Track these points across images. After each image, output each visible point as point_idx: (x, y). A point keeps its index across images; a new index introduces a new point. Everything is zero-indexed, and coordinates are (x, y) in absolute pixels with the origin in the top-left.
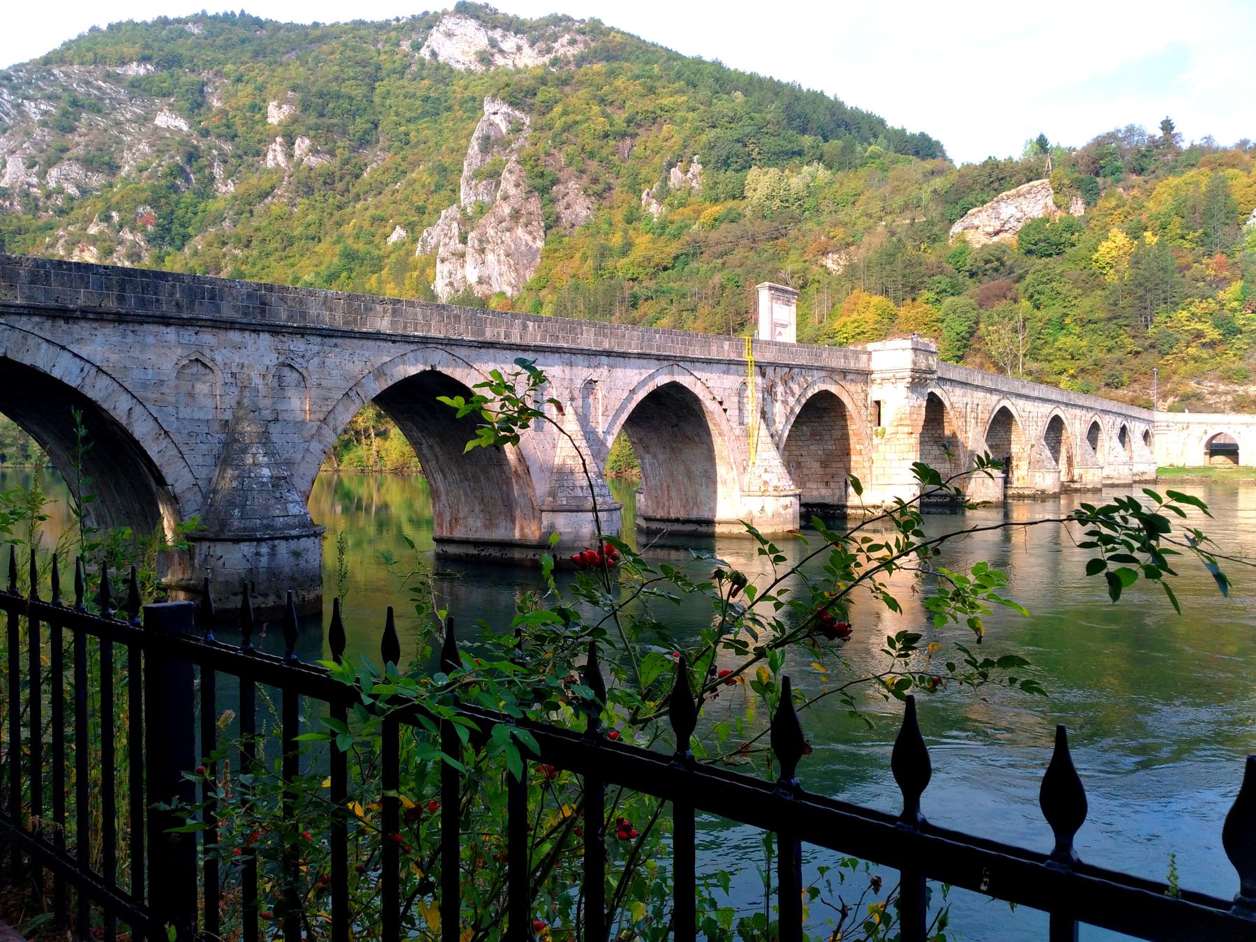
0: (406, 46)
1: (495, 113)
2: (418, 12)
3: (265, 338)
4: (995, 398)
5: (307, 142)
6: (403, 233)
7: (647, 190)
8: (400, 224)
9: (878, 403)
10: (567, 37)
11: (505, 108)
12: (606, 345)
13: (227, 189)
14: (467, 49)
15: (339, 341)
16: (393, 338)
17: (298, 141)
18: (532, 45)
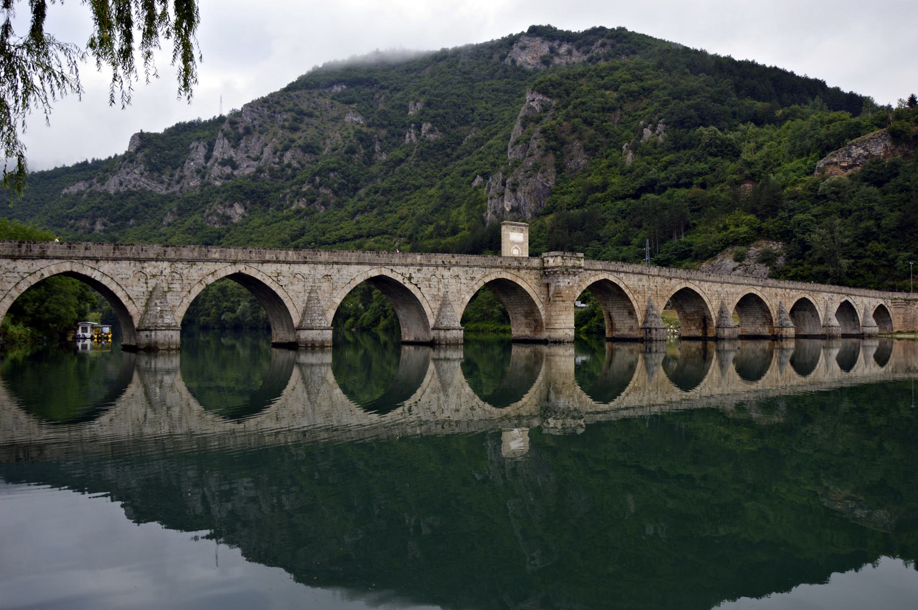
1: (533, 100)
2: (506, 35)
3: (166, 264)
5: (429, 125)
6: (482, 180)
7: (626, 144)
8: (479, 174)
9: (548, 285)
10: (600, 41)
11: (540, 97)
12: (335, 259)
14: (535, 56)
17: (424, 125)
18: (578, 49)
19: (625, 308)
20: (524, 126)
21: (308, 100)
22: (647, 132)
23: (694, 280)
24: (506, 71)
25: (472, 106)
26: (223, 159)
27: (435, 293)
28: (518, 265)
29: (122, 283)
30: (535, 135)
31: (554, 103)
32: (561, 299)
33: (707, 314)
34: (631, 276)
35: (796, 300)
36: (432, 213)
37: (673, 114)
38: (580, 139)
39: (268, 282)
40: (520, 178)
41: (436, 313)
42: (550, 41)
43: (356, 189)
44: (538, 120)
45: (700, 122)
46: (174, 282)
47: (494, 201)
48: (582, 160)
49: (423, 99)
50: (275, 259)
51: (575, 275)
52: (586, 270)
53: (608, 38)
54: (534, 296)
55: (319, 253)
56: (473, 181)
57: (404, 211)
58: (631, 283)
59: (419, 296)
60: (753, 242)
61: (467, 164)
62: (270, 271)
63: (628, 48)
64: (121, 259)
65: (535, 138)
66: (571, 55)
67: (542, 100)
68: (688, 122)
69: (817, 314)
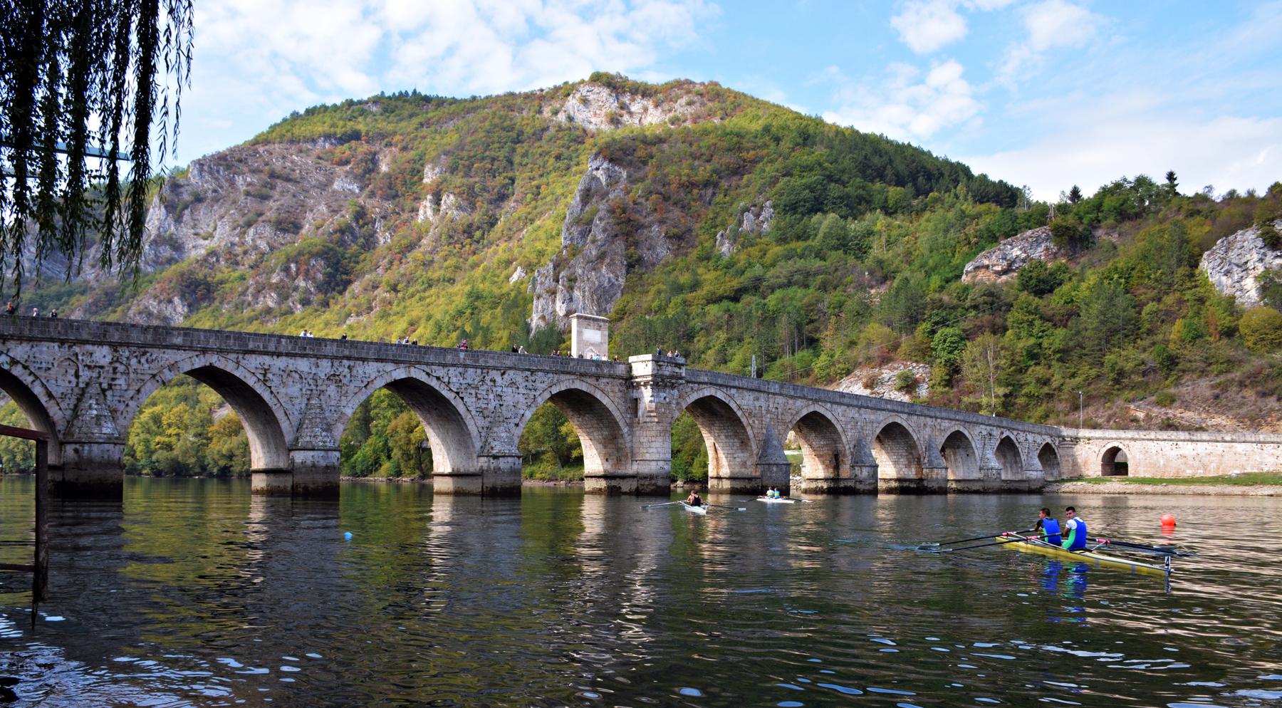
0: (547, 112)
1: (597, 169)
2: (559, 83)
3: (106, 350)
4: (799, 403)
5: (452, 197)
6: (523, 274)
8: (521, 265)
9: (636, 399)
10: (683, 101)
11: (605, 165)
12: (347, 353)
13: (384, 238)
15: (150, 350)
17: (444, 198)
18: (656, 106)
19: (736, 435)
21: (284, 157)
23: (825, 401)
25: (510, 174)
26: (159, 235)
27: (484, 406)
28: (595, 370)
29: (41, 374)
30: (601, 214)
33: (840, 447)
34: (745, 393)
35: (949, 433)
36: (454, 318)
37: (782, 195)
38: (662, 222)
39: (251, 381)
40: (580, 271)
43: (349, 282)
46: (118, 375)
47: (542, 301)
48: (663, 251)
50: (261, 348)
51: (673, 387)
52: (688, 382)
54: (617, 415)
57: (416, 311)
58: (744, 402)
59: (461, 409)
60: (887, 363)
62: (253, 365)
64: (41, 340)
69: (974, 453)
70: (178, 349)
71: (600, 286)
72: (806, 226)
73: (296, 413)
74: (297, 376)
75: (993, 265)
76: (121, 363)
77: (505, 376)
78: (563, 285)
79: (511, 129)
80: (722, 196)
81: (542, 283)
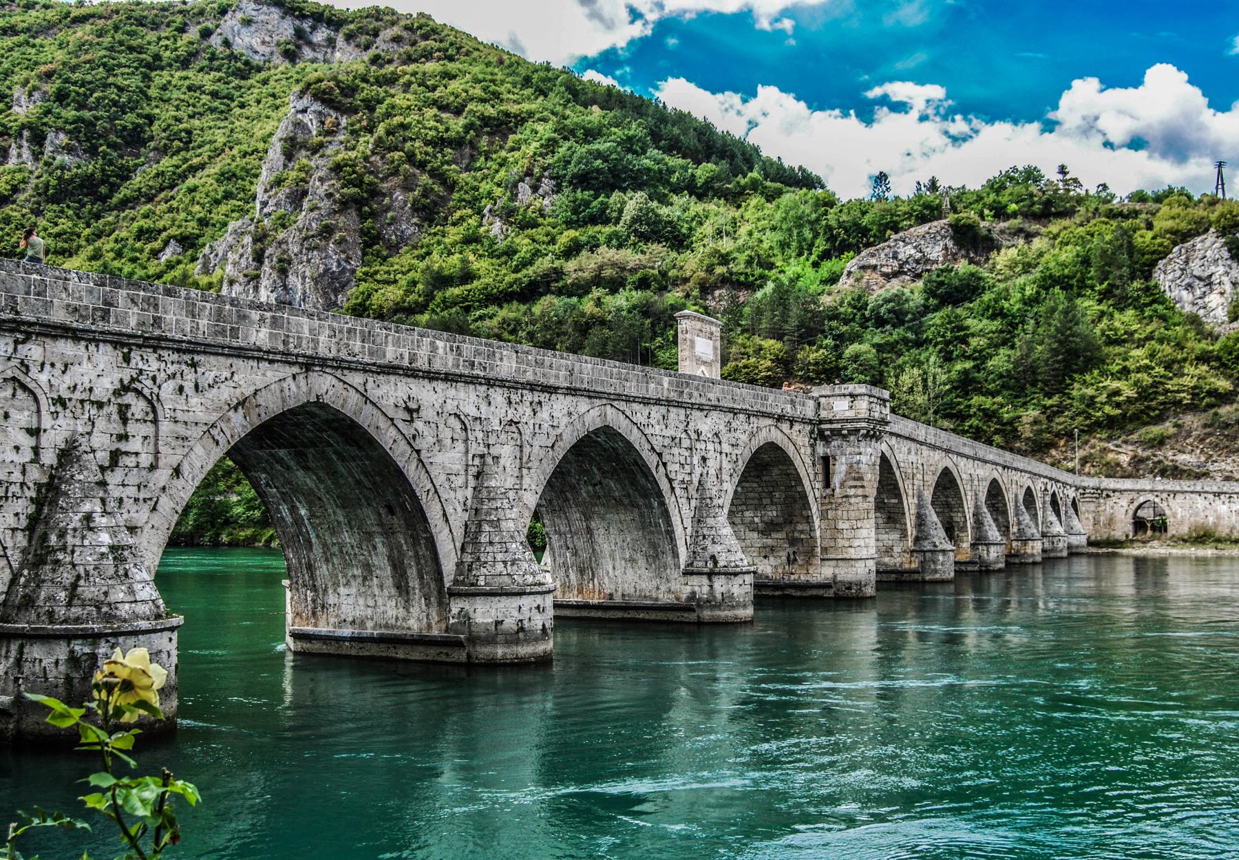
1: (304, 111)
3: (105, 356)
4: (938, 455)
5: (62, 136)
6: (179, 250)
9: (826, 461)
11: (317, 106)
12: (529, 377)
14: (267, 39)
16: (271, 357)
18: (349, 37)
20: (289, 156)
22: (524, 188)
23: (954, 452)
24: (213, 57)
25: (147, 110)
30: (321, 174)
31: (344, 121)
32: (860, 491)
33: (957, 518)
38: (407, 187)
39: (387, 437)
41: (689, 531)
42: (297, 17)
44: (316, 149)
45: (611, 180)
46: (132, 428)
49: (51, 88)
50: (406, 363)
53: (407, 28)
55: (498, 355)
56: (162, 250)
59: (664, 485)
61: (146, 216)
62: (392, 401)
63: (439, 50)
65: (321, 180)
66: (334, 48)
67: (320, 113)
68: (596, 179)
70: (259, 359)
71: (326, 271)
72: (605, 206)
73: (459, 509)
74: (458, 426)
75: (882, 266)
76: (139, 393)
77: (709, 420)
78: (272, 268)
79: (140, 50)
80: (482, 159)
81: (235, 264)
